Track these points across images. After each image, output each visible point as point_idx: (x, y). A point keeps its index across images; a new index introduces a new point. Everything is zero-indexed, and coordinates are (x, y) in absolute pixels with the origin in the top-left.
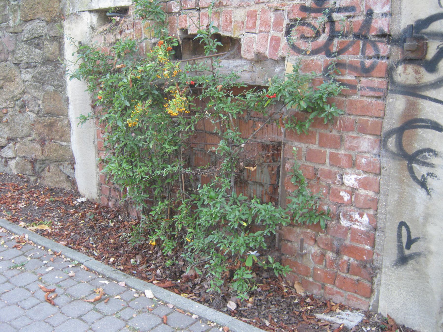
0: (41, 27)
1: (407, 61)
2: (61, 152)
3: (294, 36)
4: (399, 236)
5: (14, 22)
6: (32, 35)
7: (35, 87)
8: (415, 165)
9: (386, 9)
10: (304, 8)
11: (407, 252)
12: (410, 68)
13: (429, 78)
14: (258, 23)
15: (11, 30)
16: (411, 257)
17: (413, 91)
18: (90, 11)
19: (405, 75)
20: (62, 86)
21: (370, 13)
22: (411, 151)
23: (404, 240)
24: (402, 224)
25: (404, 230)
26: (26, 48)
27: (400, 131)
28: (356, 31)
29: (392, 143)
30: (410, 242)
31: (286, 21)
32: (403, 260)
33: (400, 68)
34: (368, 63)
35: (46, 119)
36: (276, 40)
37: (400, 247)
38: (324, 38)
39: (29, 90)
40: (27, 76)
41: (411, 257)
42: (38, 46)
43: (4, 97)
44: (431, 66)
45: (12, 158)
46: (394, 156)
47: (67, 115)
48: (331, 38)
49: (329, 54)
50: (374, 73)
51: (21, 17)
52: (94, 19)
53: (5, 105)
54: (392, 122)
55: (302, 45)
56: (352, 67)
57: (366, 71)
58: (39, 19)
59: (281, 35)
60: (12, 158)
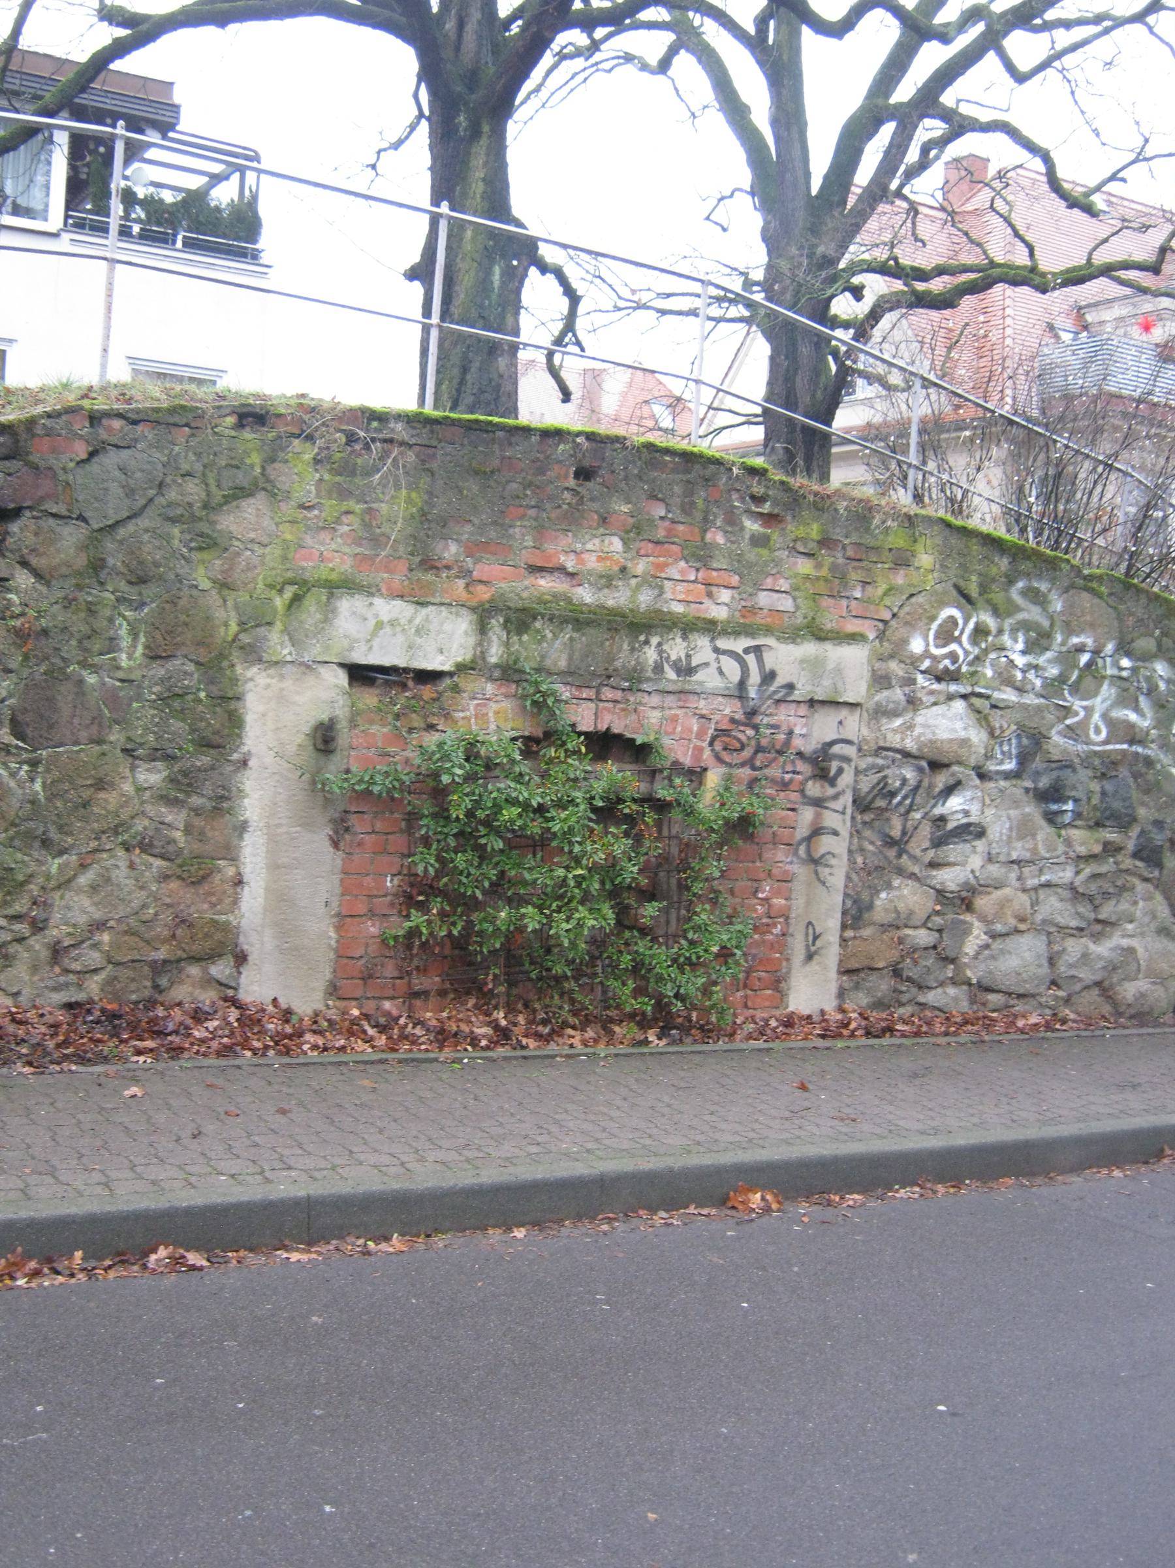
0: (186, 673)
1: (814, 777)
2: (218, 936)
3: (718, 746)
4: (807, 934)
5: (130, 657)
6: (169, 690)
7: (173, 802)
8: (820, 869)
9: (804, 731)
10: (733, 721)
11: (813, 949)
12: (818, 785)
13: (830, 791)
14: (679, 729)
15: (121, 674)
16: (816, 953)
17: (818, 803)
18: (342, 665)
19: (814, 789)
20: (228, 799)
21: (790, 733)
22: (817, 855)
23: (811, 938)
24: (810, 923)
25: (811, 931)
26: (153, 716)
27: (809, 839)
28: (778, 747)
29: (802, 850)
30: (816, 938)
31: (711, 731)
32: (810, 957)
33: (810, 783)
34: (787, 777)
35: (193, 869)
36: (700, 750)
37: (807, 946)
38: (747, 753)
39: (148, 808)
40: (152, 776)
41: (816, 953)
42: (181, 714)
43: (96, 825)
44: (832, 782)
45: (95, 971)
46: (804, 862)
47: (234, 860)
48: (756, 752)
49: (754, 768)
50: (792, 787)
51: (147, 647)
52: (342, 678)
53: (93, 844)
54: (802, 831)
55: (727, 757)
56: (773, 781)
57: (785, 786)
58: (186, 656)
59: (705, 744)
60: (95, 971)
